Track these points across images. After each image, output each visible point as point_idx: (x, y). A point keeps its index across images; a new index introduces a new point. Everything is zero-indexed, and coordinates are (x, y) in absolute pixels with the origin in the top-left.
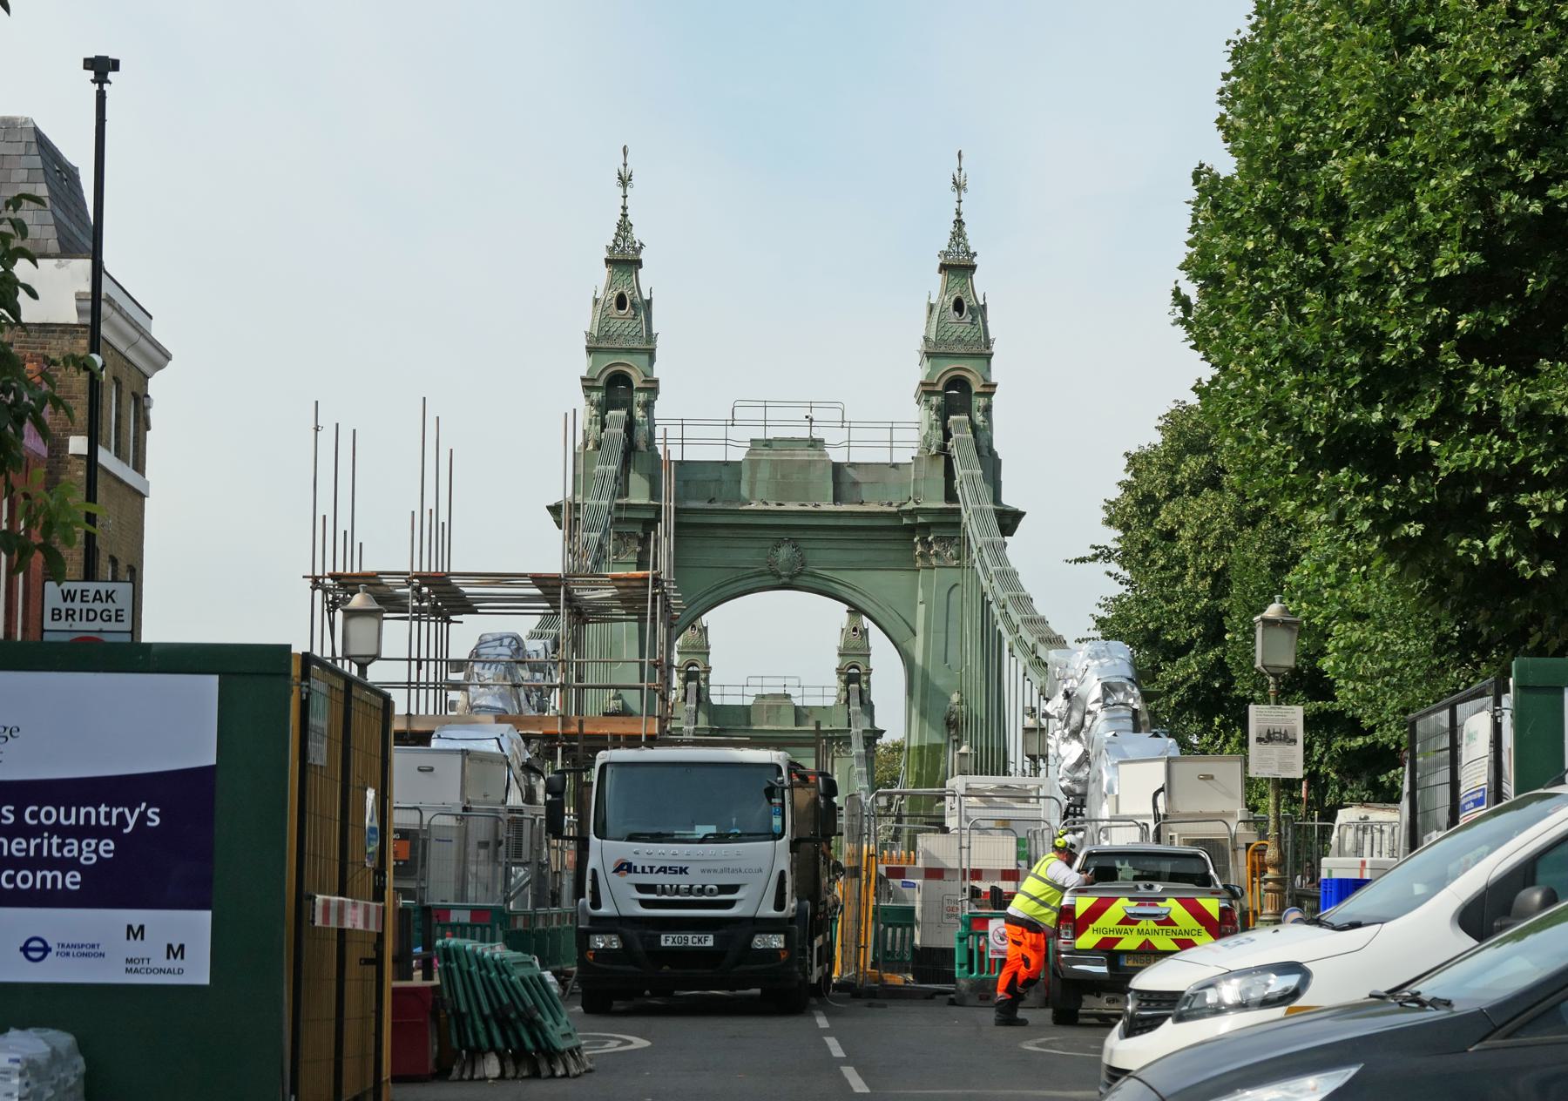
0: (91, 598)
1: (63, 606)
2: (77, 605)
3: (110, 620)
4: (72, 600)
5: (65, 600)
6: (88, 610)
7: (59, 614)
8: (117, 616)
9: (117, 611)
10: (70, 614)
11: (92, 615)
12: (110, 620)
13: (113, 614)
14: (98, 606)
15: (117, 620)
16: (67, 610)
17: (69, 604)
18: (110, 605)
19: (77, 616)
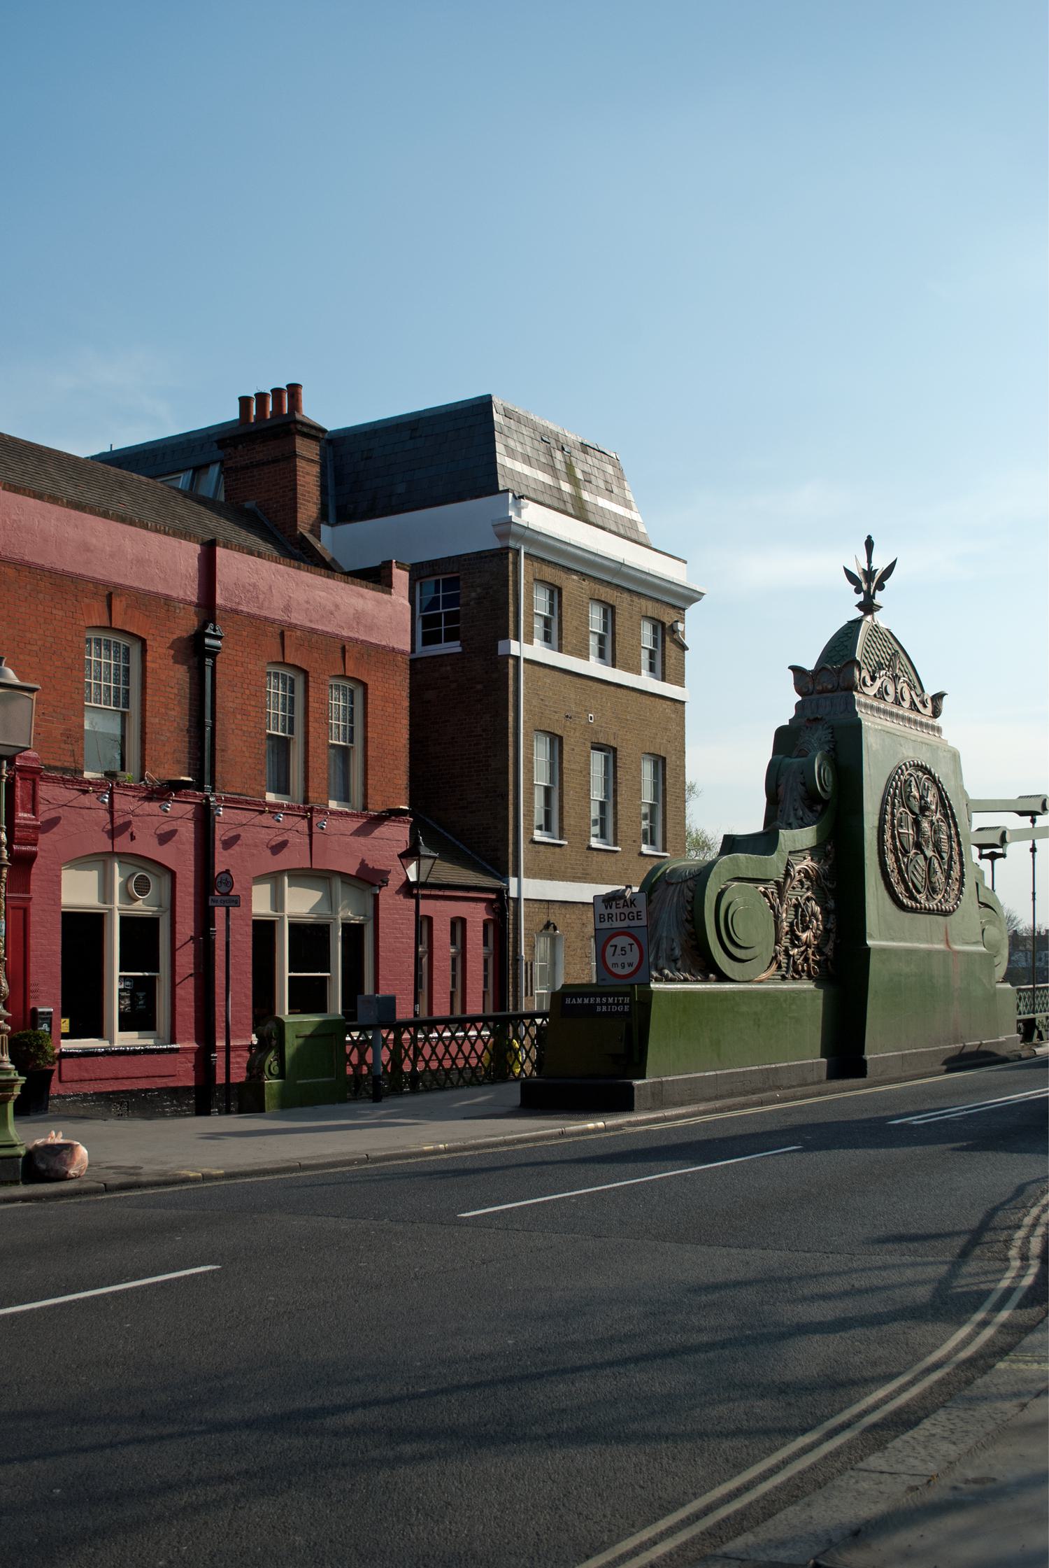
0: (621, 905)
1: (606, 912)
2: (614, 911)
3: (634, 919)
4: (611, 908)
5: (606, 908)
6: (621, 914)
7: (604, 918)
8: (638, 915)
9: (638, 912)
10: (610, 917)
11: (623, 917)
12: (634, 919)
13: (635, 915)
14: (626, 910)
15: (638, 919)
16: (608, 914)
17: (609, 911)
18: (634, 910)
19: (614, 918)
